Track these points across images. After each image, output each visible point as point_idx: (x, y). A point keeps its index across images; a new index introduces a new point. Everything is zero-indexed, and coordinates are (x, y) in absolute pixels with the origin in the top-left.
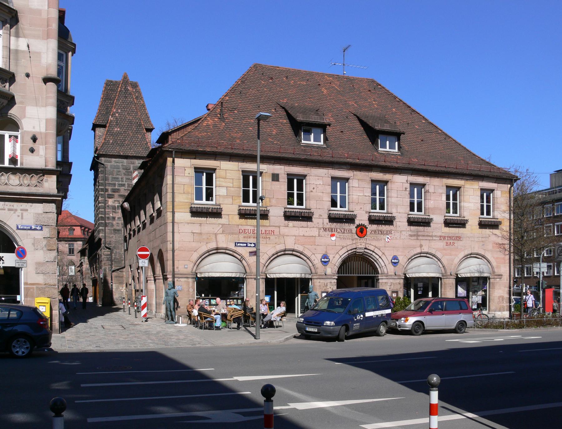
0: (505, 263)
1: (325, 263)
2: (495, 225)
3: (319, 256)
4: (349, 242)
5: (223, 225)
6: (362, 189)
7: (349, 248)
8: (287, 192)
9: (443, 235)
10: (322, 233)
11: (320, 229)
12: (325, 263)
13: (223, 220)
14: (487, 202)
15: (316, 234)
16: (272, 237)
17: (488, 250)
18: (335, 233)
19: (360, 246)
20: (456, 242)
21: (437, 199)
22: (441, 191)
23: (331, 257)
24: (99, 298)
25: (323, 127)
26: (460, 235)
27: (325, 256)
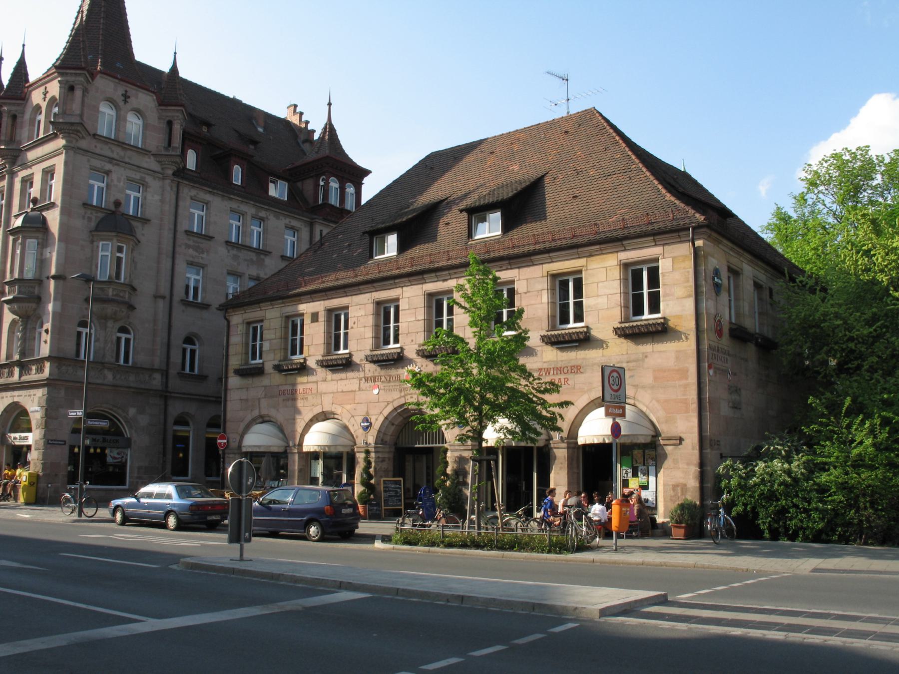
0: (687, 411)
1: (366, 429)
2: (662, 331)
3: (359, 419)
4: (396, 395)
5: (265, 387)
6: (413, 311)
7: (396, 404)
8: (584, 300)
9: (545, 366)
10: (364, 385)
11: (360, 379)
12: (366, 429)
13: (265, 381)
14: (293, 336)
15: (356, 387)
16: (310, 397)
17: (643, 387)
18: (379, 383)
19: (410, 400)
20: (570, 376)
21: (533, 302)
22: (539, 287)
23: (373, 421)
24: (294, 471)
25: (203, 266)
26: (579, 363)
27: (366, 420)
